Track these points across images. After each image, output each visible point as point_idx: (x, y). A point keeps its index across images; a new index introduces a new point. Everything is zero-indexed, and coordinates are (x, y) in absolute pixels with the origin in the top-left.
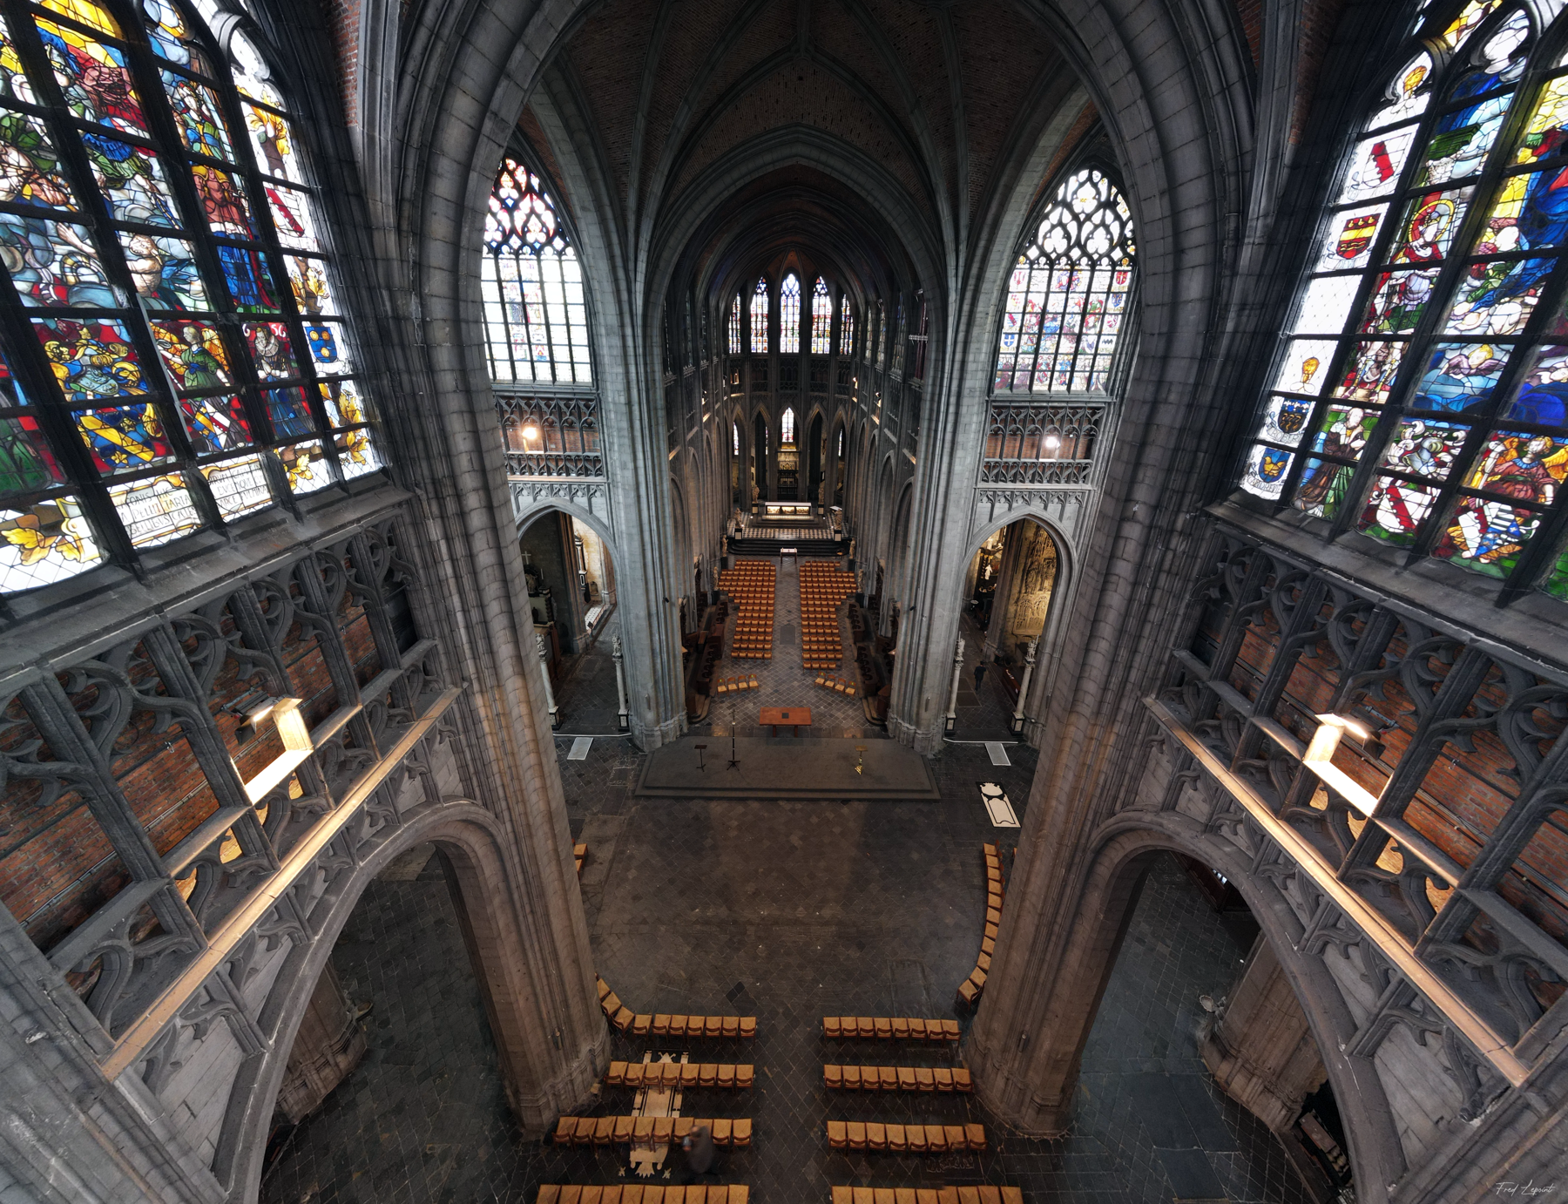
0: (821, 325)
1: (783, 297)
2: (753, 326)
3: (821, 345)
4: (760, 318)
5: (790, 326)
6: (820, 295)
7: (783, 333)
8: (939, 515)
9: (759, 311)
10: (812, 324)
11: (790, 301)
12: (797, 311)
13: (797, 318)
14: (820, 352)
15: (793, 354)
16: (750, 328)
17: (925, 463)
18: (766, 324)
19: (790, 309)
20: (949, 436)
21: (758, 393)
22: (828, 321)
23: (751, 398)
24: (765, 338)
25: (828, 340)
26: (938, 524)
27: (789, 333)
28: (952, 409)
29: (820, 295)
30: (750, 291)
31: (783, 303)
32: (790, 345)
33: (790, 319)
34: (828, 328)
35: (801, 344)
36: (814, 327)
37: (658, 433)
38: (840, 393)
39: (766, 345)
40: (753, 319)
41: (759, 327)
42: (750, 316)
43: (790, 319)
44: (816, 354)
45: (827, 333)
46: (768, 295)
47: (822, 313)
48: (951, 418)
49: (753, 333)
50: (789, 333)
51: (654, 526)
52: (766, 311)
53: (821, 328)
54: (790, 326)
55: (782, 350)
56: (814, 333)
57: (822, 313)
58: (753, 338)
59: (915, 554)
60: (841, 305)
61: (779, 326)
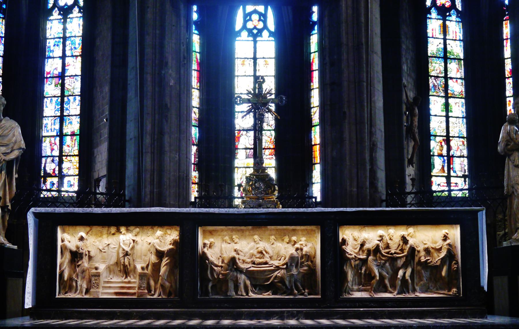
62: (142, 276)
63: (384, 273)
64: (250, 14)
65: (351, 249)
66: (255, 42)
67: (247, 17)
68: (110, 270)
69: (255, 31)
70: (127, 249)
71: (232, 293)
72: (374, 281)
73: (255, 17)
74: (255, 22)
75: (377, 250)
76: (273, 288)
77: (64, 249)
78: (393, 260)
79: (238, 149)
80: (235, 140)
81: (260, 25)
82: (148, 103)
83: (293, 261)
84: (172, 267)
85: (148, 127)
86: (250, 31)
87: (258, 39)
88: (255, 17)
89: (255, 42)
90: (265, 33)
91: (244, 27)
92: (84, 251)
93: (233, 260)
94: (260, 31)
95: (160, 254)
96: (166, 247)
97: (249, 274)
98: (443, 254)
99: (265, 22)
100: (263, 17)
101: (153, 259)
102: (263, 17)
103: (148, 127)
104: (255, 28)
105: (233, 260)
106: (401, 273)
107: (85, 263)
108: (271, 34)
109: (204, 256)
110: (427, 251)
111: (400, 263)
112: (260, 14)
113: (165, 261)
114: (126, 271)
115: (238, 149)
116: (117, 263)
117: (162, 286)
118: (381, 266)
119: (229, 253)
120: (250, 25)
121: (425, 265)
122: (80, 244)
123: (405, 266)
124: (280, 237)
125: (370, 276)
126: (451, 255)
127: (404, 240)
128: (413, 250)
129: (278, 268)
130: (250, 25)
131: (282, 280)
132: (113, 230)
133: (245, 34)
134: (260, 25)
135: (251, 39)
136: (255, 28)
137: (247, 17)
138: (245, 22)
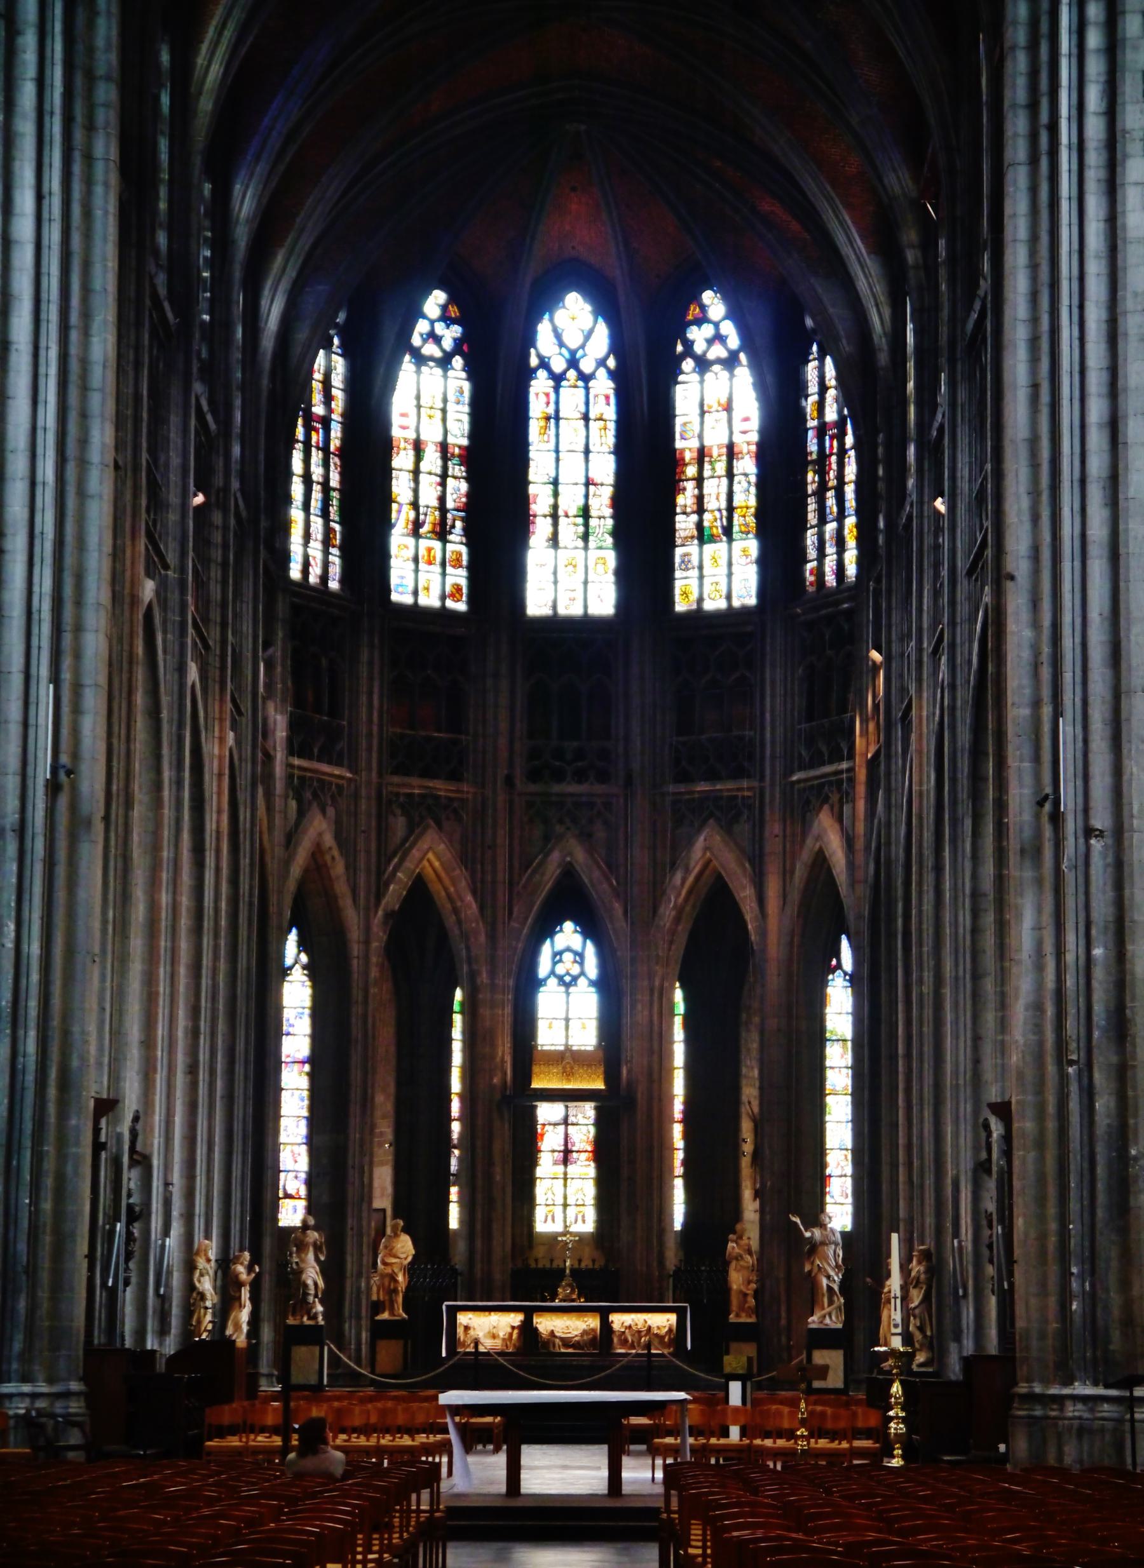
0: (715, 490)
1: (540, 384)
2: (401, 487)
3: (715, 574)
4: (432, 460)
5: (571, 500)
6: (703, 365)
7: (541, 529)
8: (1097, 410)
9: (432, 434)
10: (673, 488)
11: (571, 399)
12: (604, 438)
13: (605, 468)
14: (714, 604)
15: (586, 625)
16: (386, 498)
17: (1033, 253)
18: (458, 489)
19: (572, 433)
20: (1095, 128)
21: (416, 786)
22: (747, 466)
23: (384, 805)
24: (457, 545)
25: (748, 547)
26: (1097, 440)
27: (569, 531)
28: (1094, 39)
29: (703, 365)
30: (389, 333)
31: (537, 407)
32: (571, 581)
33: (572, 470)
34: (746, 497)
35: (623, 575)
36: (686, 499)
37: (89, 158)
38: (817, 760)
39: (459, 577)
40: (402, 460)
41: (429, 496)
42: (386, 447)
43: (572, 470)
44: (698, 616)
45: (745, 519)
46: (473, 372)
47: (716, 439)
48: (1095, 67)
49: (401, 517)
50: (569, 531)
51: (47, 470)
52: (459, 435)
53: (715, 498)
54: (571, 500)
55: (537, 604)
56: (685, 524)
57: (716, 439)
58: (400, 543)
59: (1035, 604)
60: (801, 389)
61: (523, 501)
62: (504, 1340)
63: (635, 1340)
64: (560, 953)
65: (616, 1326)
66: (568, 994)
67: (557, 956)
68: (485, 1336)
69: (567, 979)
70: (495, 1324)
71: (552, 1349)
72: (628, 1344)
73: (568, 957)
74: (568, 965)
75: (630, 1327)
76: (574, 1346)
77: (461, 1324)
78: (639, 1332)
79: (541, 1151)
80: (536, 1138)
81: (575, 970)
82: (479, 1196)
83: (585, 1332)
84: (520, 1335)
85: (479, 1215)
86: (561, 979)
87: (572, 989)
88: (568, 957)
89: (568, 994)
90: (582, 981)
91: (553, 973)
92: (471, 1325)
93: (552, 1332)
94: (575, 979)
95: (513, 1328)
96: (517, 1323)
97: (562, 1339)
98: (666, 1329)
99: (582, 964)
100: (580, 957)
101: (509, 1330)
102: (580, 957)
103: (479, 1215)
104: (568, 973)
105: (552, 1332)
106: (643, 1339)
107: (471, 1332)
108: (592, 983)
109: (536, 1329)
110: (658, 1328)
111: (643, 1334)
112: (576, 953)
113: (516, 1331)
114: (494, 1337)
115: (541, 1151)
116: (489, 1332)
117: (514, 1345)
118: (633, 1335)
119: (550, 1328)
120: (560, 969)
121: (657, 1335)
122: (469, 1321)
123: (646, 1335)
124: (578, 1319)
125: (626, 1340)
126: (670, 1330)
127: (646, 1322)
128: (650, 1327)
129: (576, 1336)
130: (560, 969)
131: (578, 1342)
132: (487, 1313)
133: (553, 982)
134: (575, 970)
135: (563, 989)
136: (568, 973)
137: (557, 956)
138: (555, 964)
